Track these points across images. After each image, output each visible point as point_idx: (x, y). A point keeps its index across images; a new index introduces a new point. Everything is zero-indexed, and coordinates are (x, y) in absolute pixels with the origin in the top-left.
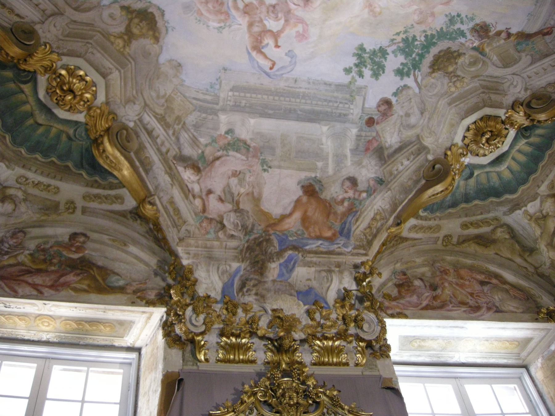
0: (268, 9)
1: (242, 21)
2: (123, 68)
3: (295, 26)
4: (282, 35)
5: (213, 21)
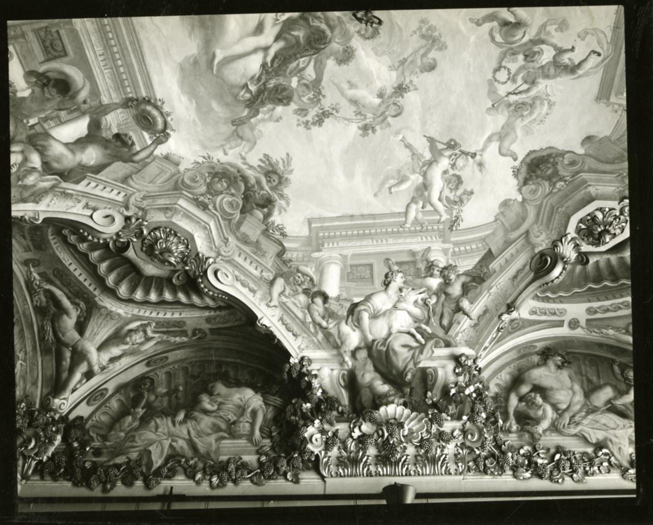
0: (529, 62)
1: (543, 85)
2: (587, 182)
3: (549, 33)
4: (559, 45)
5: (542, 110)
